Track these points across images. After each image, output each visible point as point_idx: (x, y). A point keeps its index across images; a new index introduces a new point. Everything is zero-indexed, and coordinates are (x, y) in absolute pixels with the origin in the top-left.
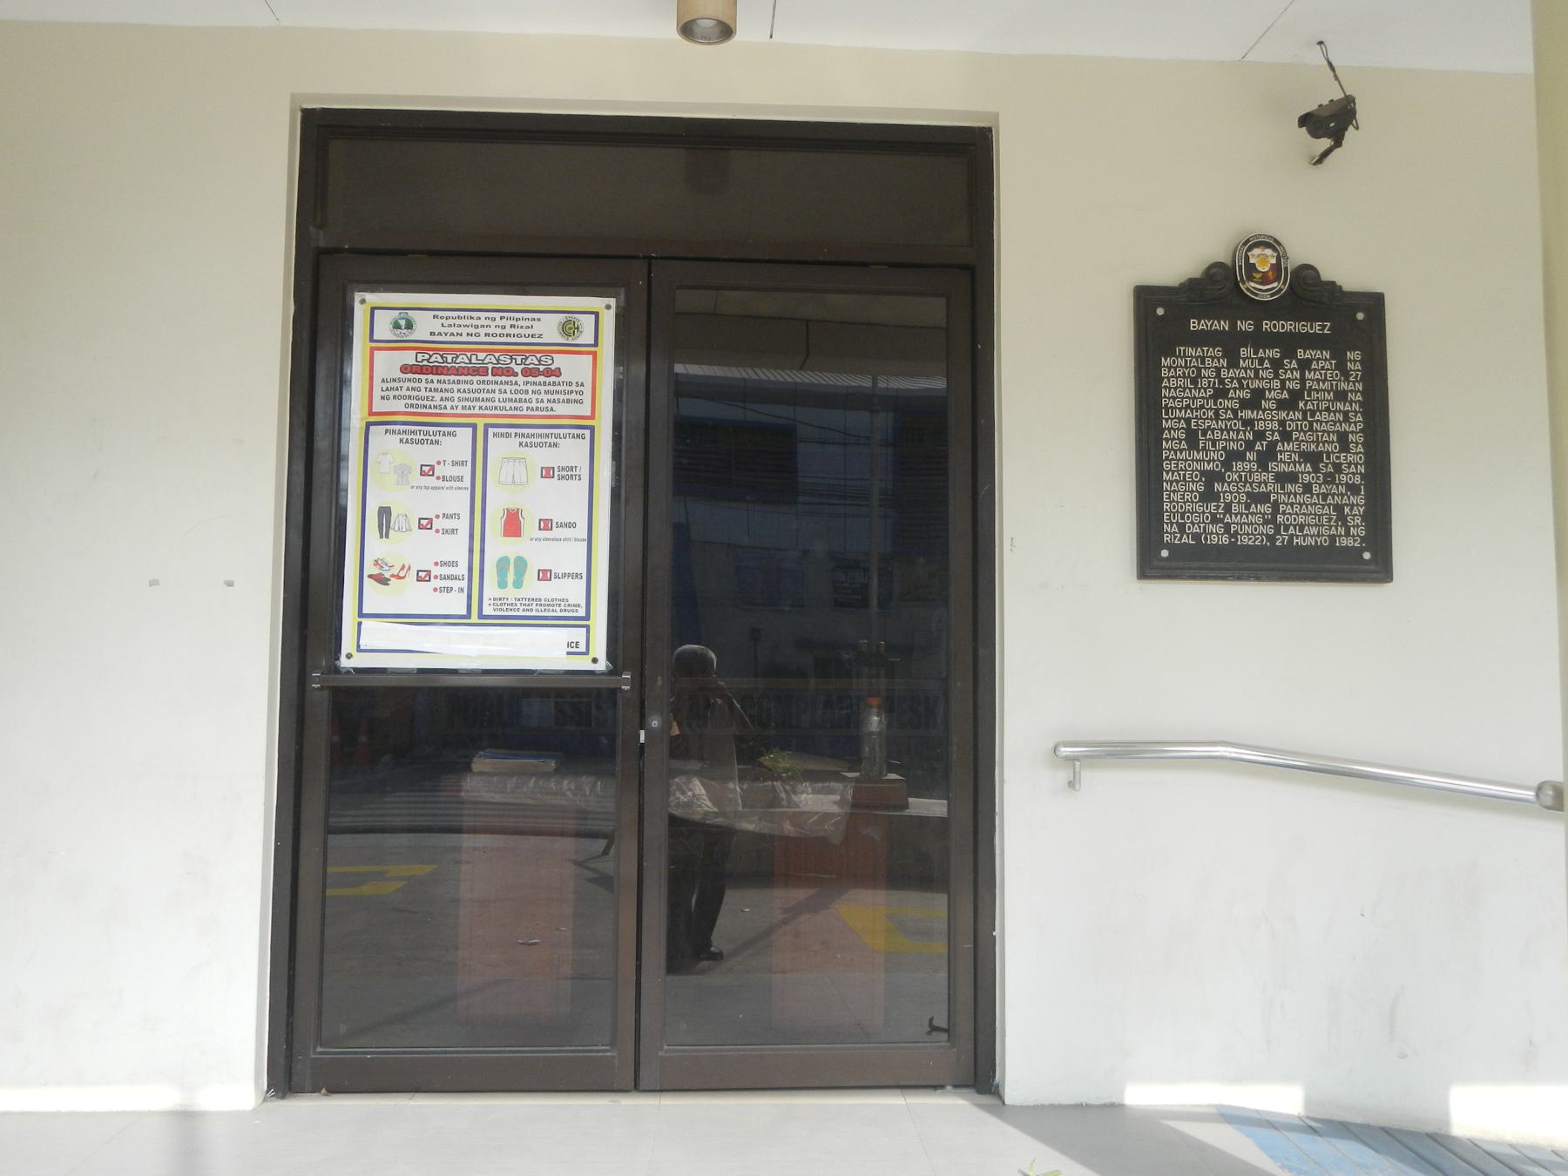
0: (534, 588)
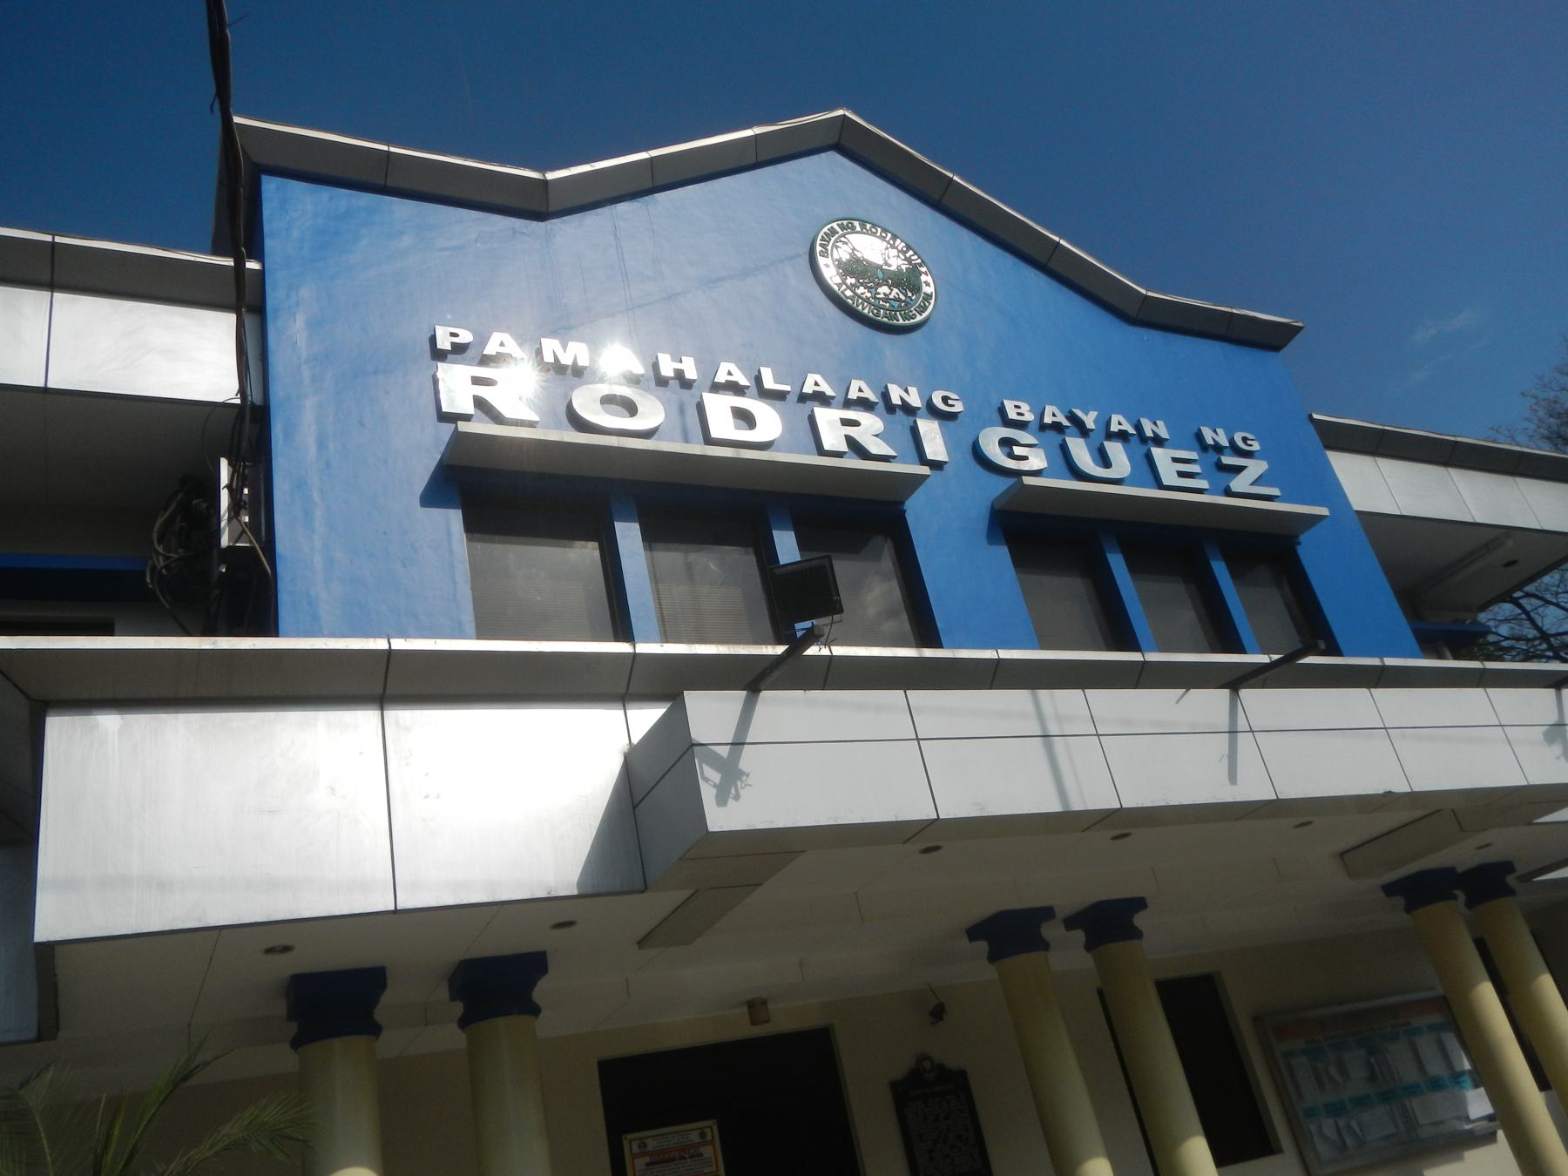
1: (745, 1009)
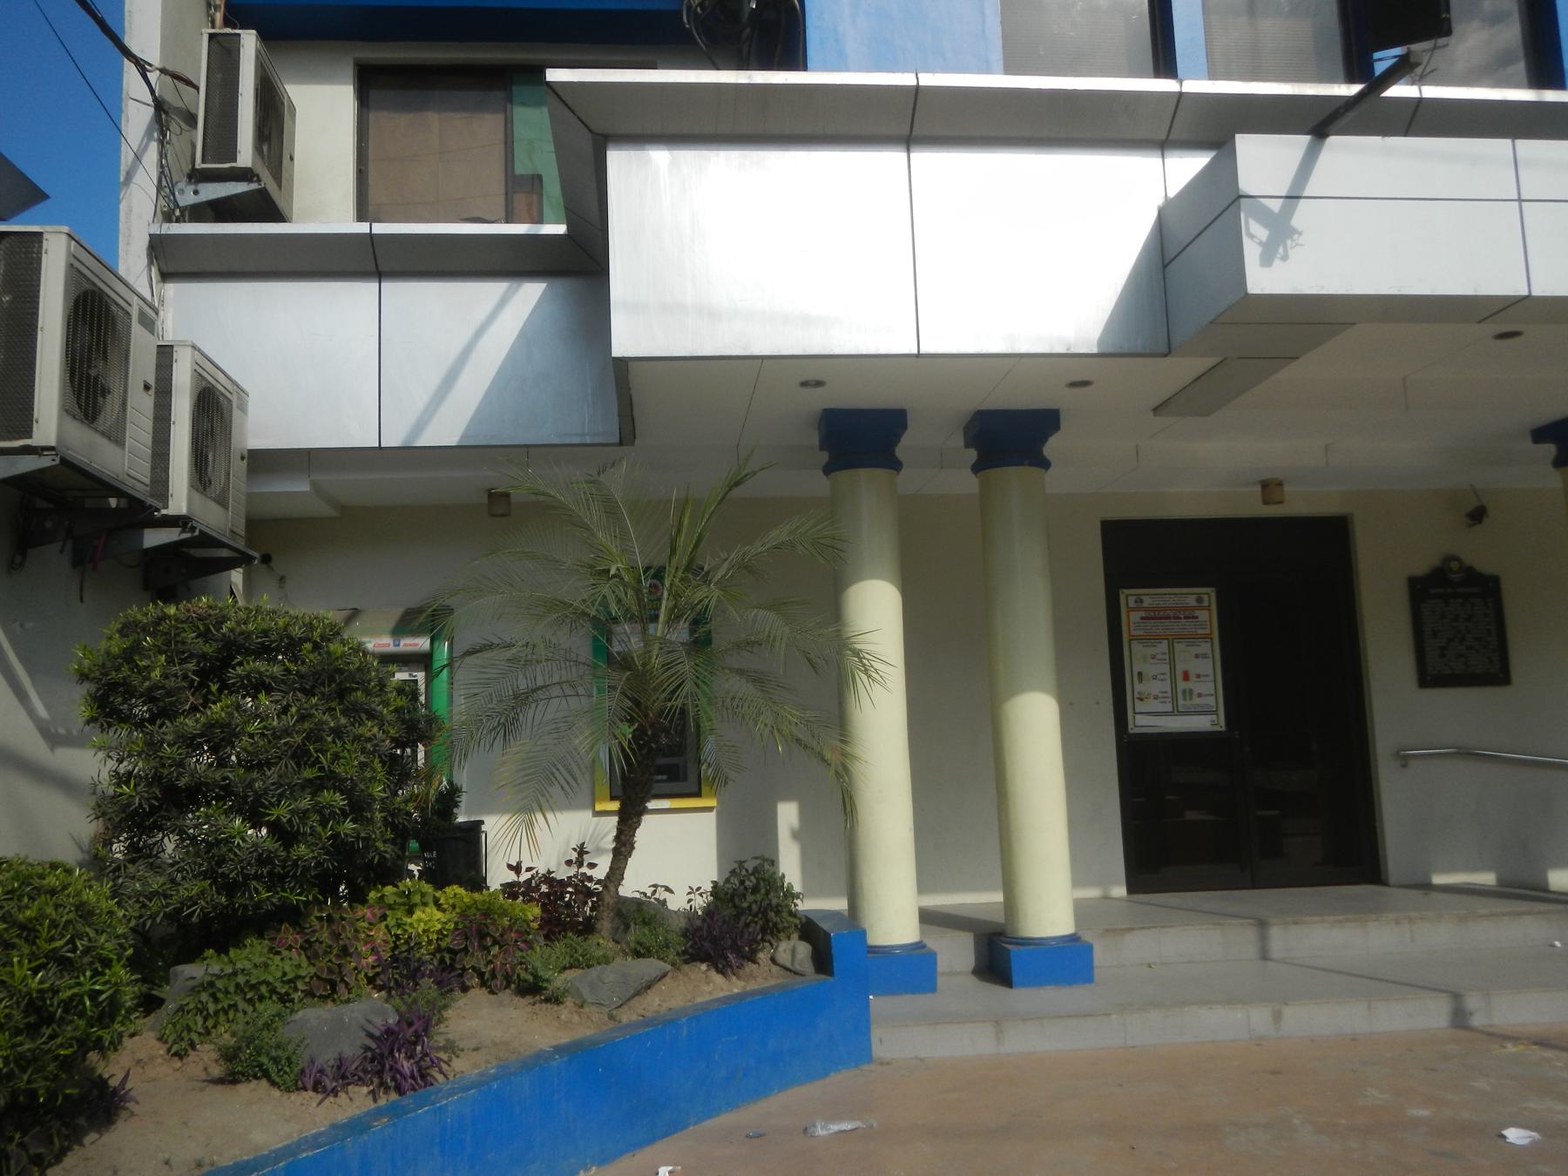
0: (1197, 701)
1: (1258, 489)
